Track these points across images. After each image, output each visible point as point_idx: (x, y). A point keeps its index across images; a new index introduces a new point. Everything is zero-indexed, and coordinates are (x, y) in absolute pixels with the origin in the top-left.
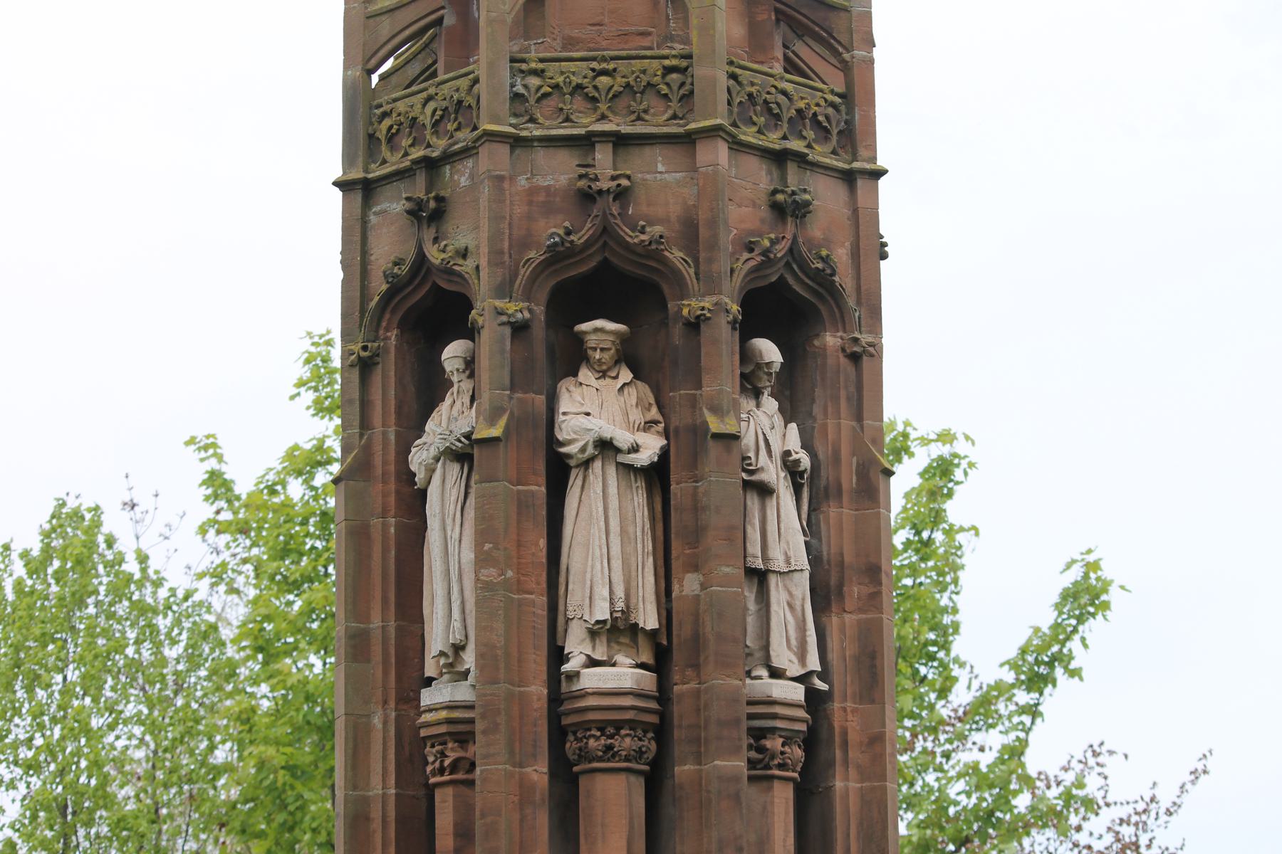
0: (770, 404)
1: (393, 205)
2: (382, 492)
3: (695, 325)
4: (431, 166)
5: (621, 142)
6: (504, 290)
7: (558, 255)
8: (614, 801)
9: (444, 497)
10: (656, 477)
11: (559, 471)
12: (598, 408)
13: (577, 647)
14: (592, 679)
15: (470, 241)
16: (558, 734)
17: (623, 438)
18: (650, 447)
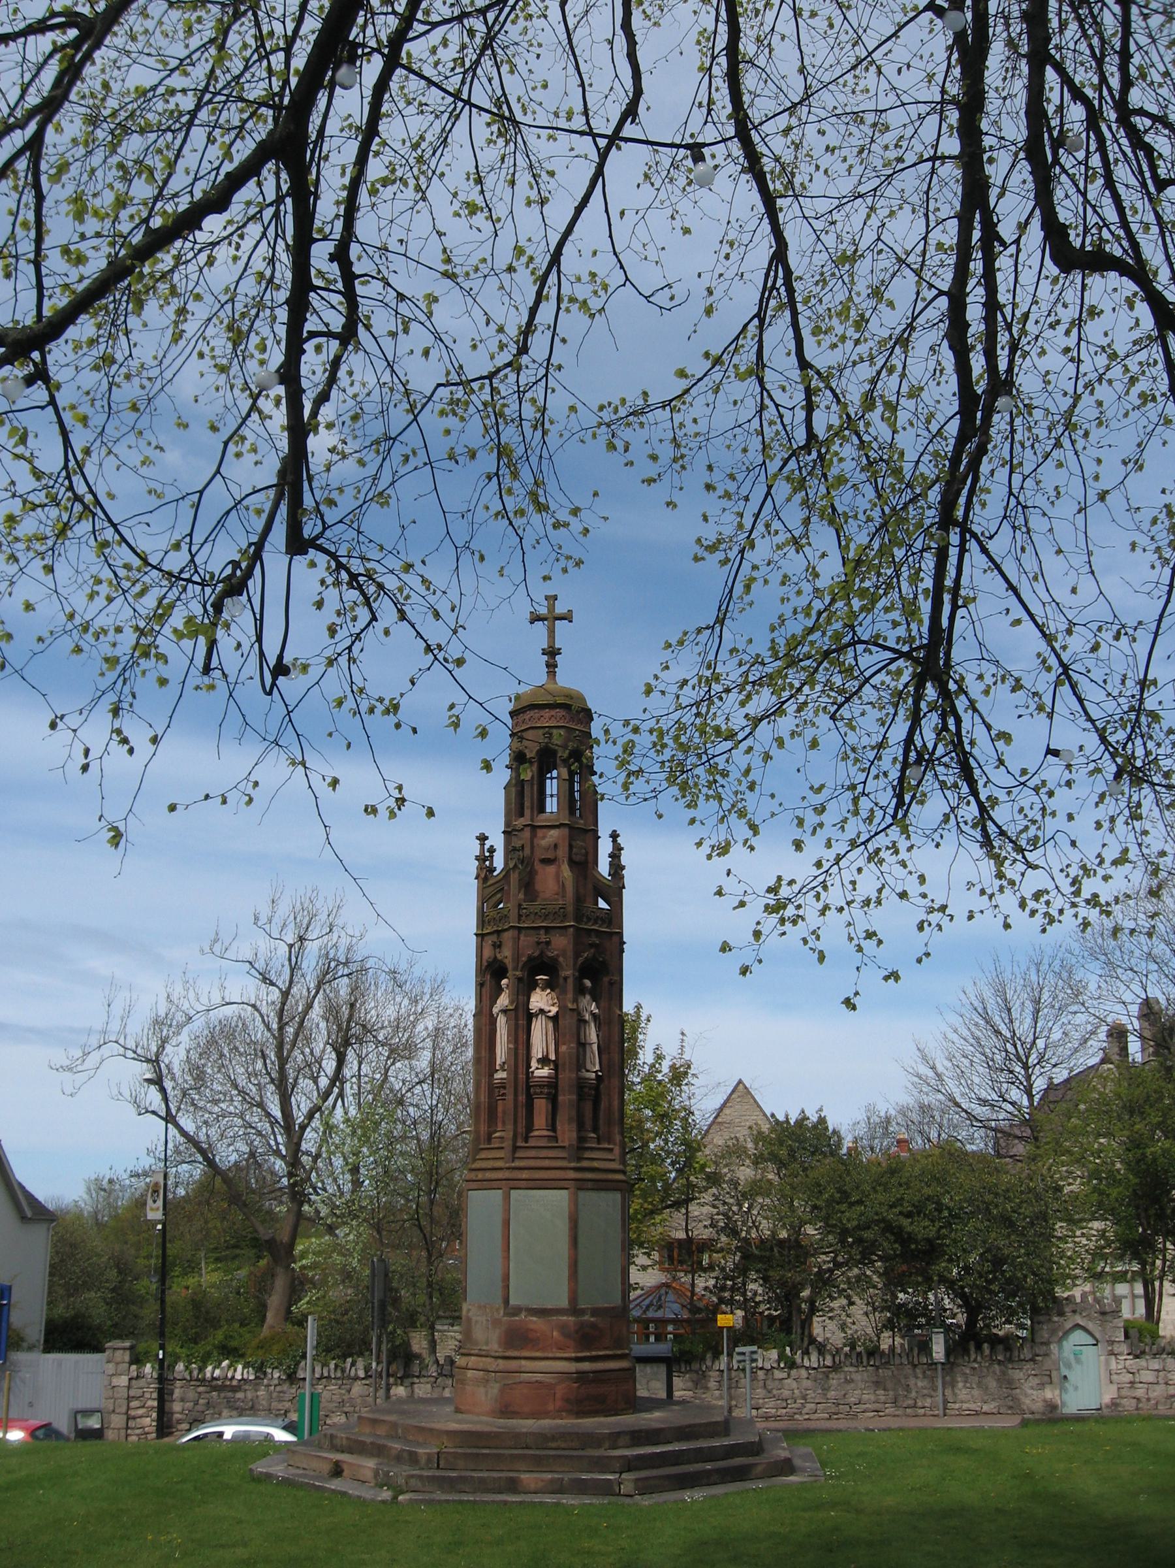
0: (588, 997)
1: (489, 941)
2: (485, 1020)
3: (565, 979)
4: (498, 932)
5: (547, 929)
6: (515, 969)
7: (531, 959)
8: (541, 1106)
9: (501, 1021)
10: (555, 1019)
11: (530, 1017)
12: (540, 1000)
13: (534, 1064)
14: (538, 1073)
15: (506, 954)
16: (528, 1087)
17: (547, 1008)
18: (554, 1010)
